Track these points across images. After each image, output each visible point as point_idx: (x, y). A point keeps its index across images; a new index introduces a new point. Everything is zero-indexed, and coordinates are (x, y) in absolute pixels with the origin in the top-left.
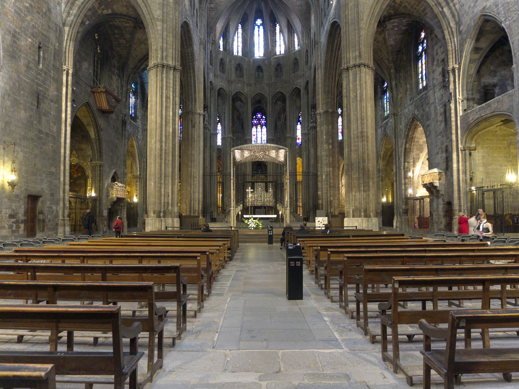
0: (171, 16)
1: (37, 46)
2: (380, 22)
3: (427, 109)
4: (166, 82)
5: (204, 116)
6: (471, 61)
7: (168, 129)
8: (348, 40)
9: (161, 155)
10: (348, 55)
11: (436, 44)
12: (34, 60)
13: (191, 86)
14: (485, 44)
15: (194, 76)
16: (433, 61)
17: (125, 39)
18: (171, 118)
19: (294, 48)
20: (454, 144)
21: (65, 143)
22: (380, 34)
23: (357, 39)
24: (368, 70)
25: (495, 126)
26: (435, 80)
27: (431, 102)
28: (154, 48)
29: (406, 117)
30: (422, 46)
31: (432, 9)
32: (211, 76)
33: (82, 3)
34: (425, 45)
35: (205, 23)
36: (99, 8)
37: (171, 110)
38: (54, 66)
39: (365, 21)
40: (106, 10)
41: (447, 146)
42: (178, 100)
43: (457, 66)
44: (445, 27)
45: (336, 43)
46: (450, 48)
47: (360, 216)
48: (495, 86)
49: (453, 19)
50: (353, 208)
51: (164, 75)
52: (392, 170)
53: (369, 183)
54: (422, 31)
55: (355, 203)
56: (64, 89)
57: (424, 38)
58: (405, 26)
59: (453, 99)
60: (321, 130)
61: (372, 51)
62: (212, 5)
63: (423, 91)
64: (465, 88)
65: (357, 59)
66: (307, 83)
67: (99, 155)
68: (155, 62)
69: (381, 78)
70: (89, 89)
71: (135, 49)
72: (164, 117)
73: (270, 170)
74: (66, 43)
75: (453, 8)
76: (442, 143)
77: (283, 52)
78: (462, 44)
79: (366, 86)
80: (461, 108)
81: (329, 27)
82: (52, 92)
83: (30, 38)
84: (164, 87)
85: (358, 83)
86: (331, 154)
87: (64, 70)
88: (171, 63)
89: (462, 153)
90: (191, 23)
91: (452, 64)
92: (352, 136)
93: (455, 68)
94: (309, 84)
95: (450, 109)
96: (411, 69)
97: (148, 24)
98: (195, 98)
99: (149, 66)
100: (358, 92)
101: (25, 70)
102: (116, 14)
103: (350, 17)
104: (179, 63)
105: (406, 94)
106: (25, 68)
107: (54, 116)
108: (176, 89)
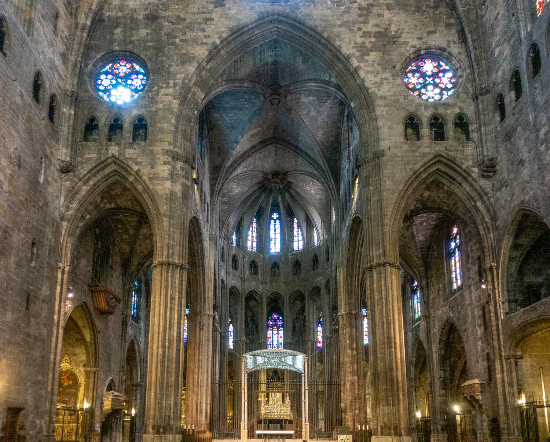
0: (179, 212)
1: (30, 242)
2: (406, 216)
3: (463, 312)
4: (172, 282)
5: (214, 318)
6: (511, 259)
7: (172, 333)
8: (370, 237)
9: (163, 362)
10: (371, 253)
11: (470, 240)
12: (26, 256)
13: (200, 285)
14: (525, 241)
15: (204, 274)
16: (468, 259)
17: (129, 234)
18: (176, 321)
19: (314, 243)
20: (497, 351)
21: (56, 347)
22: (408, 230)
23: (380, 236)
24: (393, 269)
25: (543, 331)
26: (471, 279)
27: (467, 304)
28: (159, 245)
29: (439, 320)
30: (455, 242)
31: (463, 203)
32: (223, 274)
33: (84, 197)
34: (458, 241)
35: (217, 217)
36: (101, 202)
37: (176, 312)
38: (48, 263)
39: (389, 217)
40: (108, 205)
41: (488, 354)
42: (184, 301)
43: (495, 265)
44: (479, 222)
45: (358, 239)
46: (486, 245)
47: (390, 434)
48: (540, 285)
49: (488, 214)
50: (381, 424)
51: (170, 274)
52: (427, 379)
53: (398, 395)
54: (453, 226)
55: (383, 420)
56: (58, 288)
57: (457, 234)
58: (435, 220)
59: (492, 300)
60: (343, 334)
61: (398, 249)
62: (225, 199)
63: (458, 291)
64: (505, 288)
65: (382, 257)
66: (328, 281)
67: (94, 361)
68: (160, 260)
69: (411, 276)
70: (86, 288)
71: (139, 245)
72: (168, 319)
73: (287, 379)
74: (64, 238)
75: (488, 202)
76: (483, 350)
77: (301, 247)
78: (499, 241)
79: (392, 287)
80: (502, 310)
81: (351, 223)
82: (45, 292)
83: (23, 233)
84: (170, 287)
85: (383, 283)
86: (356, 360)
87: (60, 268)
88: (177, 261)
89: (506, 362)
90: (201, 217)
91: (489, 263)
92: (378, 342)
93: (492, 267)
94: (330, 283)
95: (490, 312)
96: (443, 267)
97: (153, 220)
98: (204, 299)
99: (153, 265)
100: (384, 294)
101: (16, 268)
102: (120, 208)
103: (372, 213)
104: (186, 262)
105: (439, 294)
106: (14, 266)
107: (45, 317)
108: (182, 289)
